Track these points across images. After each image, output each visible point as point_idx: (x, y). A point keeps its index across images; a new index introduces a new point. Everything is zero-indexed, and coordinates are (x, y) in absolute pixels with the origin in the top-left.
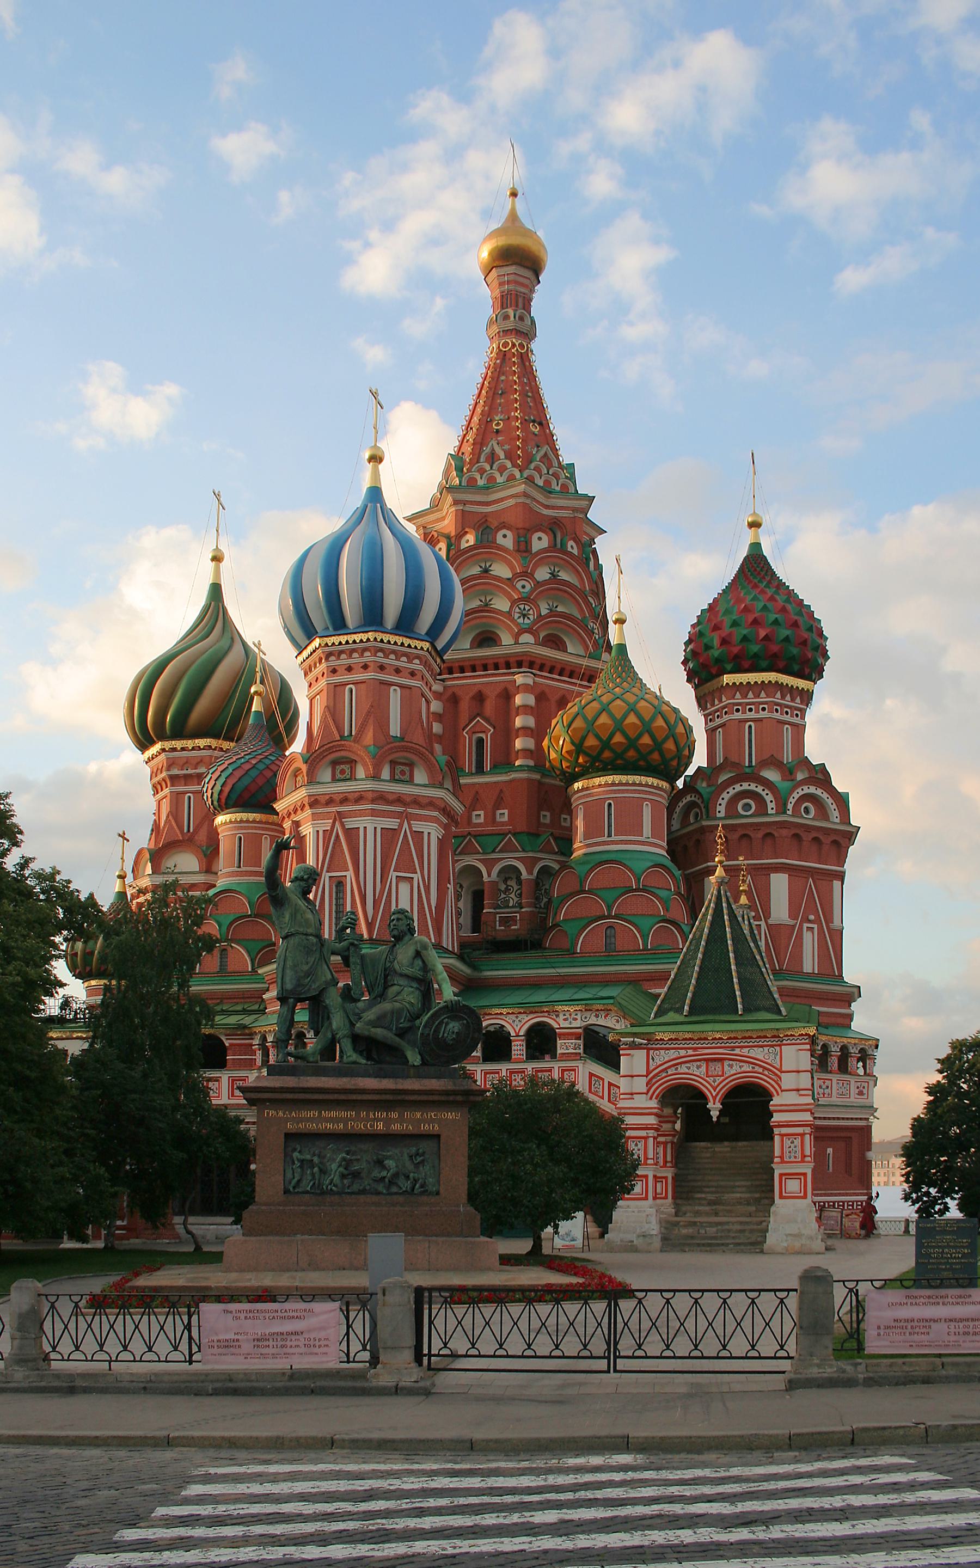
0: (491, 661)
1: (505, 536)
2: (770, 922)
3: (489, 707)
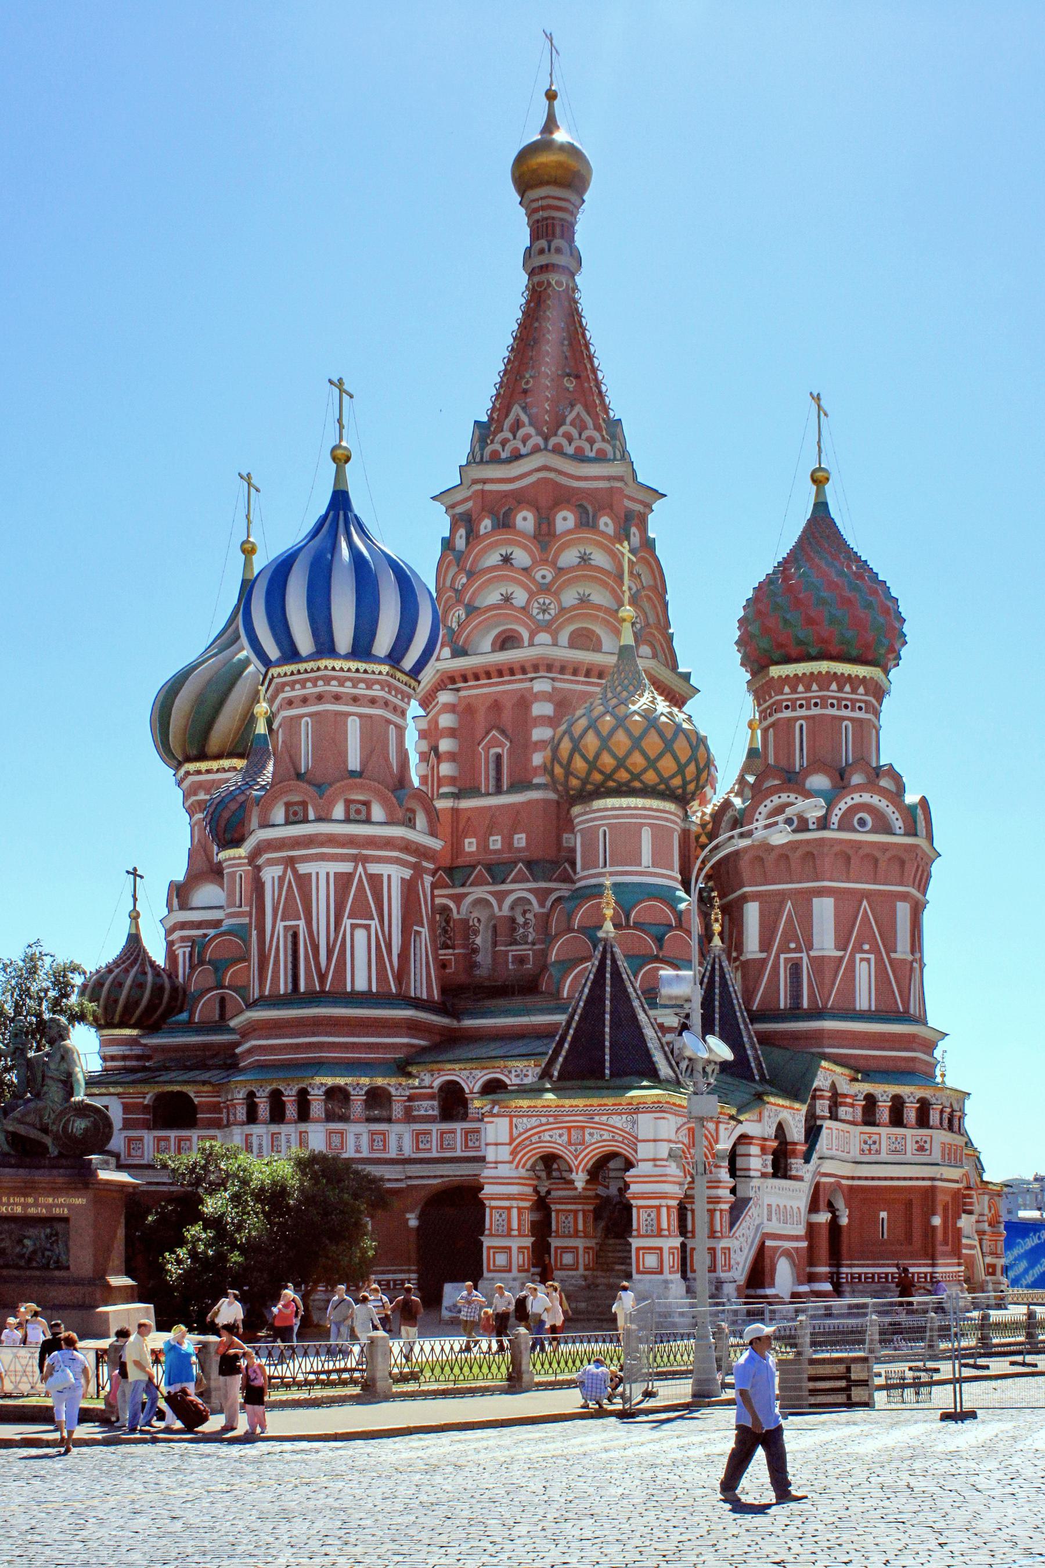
0: (505, 667)
1: (525, 519)
2: (812, 953)
3: (507, 716)
